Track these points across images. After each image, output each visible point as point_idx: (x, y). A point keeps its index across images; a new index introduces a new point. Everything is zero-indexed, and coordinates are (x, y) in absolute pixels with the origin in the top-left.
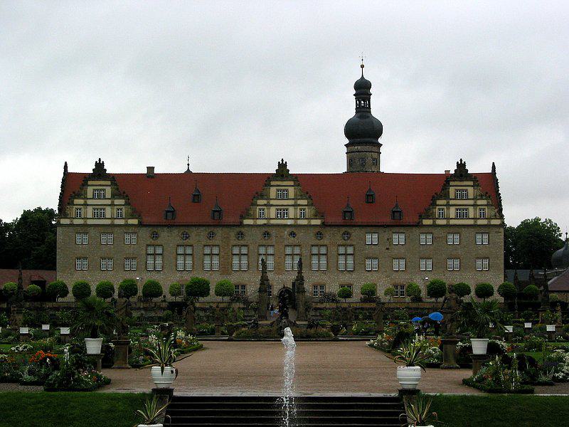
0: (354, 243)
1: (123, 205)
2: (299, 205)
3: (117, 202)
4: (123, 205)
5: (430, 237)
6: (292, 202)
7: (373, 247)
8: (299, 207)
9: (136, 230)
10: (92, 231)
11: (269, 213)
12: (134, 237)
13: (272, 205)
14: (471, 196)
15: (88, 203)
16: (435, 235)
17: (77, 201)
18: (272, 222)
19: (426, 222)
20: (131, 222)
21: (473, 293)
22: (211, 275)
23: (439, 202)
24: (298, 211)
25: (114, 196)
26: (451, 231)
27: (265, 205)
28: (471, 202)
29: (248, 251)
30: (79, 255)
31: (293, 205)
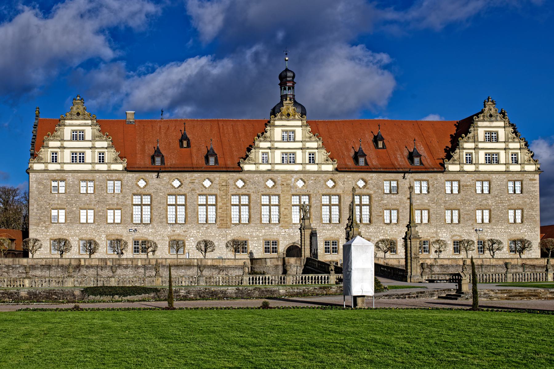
0: (372, 192)
1: (106, 148)
2: (308, 148)
3: (98, 144)
4: (106, 148)
5: (455, 184)
6: (300, 145)
7: (392, 196)
8: (308, 151)
9: (120, 176)
10: (70, 177)
11: (273, 158)
12: (118, 183)
13: (277, 148)
14: (502, 137)
15: (65, 146)
16: (461, 183)
17: (52, 144)
18: (277, 167)
19: (452, 168)
20: (114, 167)
21: (505, 249)
22: (207, 228)
23: (466, 145)
24: (307, 156)
25: (94, 139)
26: (480, 179)
27: (270, 148)
28: (503, 145)
29: (249, 202)
30: (54, 206)
31: (301, 149)
